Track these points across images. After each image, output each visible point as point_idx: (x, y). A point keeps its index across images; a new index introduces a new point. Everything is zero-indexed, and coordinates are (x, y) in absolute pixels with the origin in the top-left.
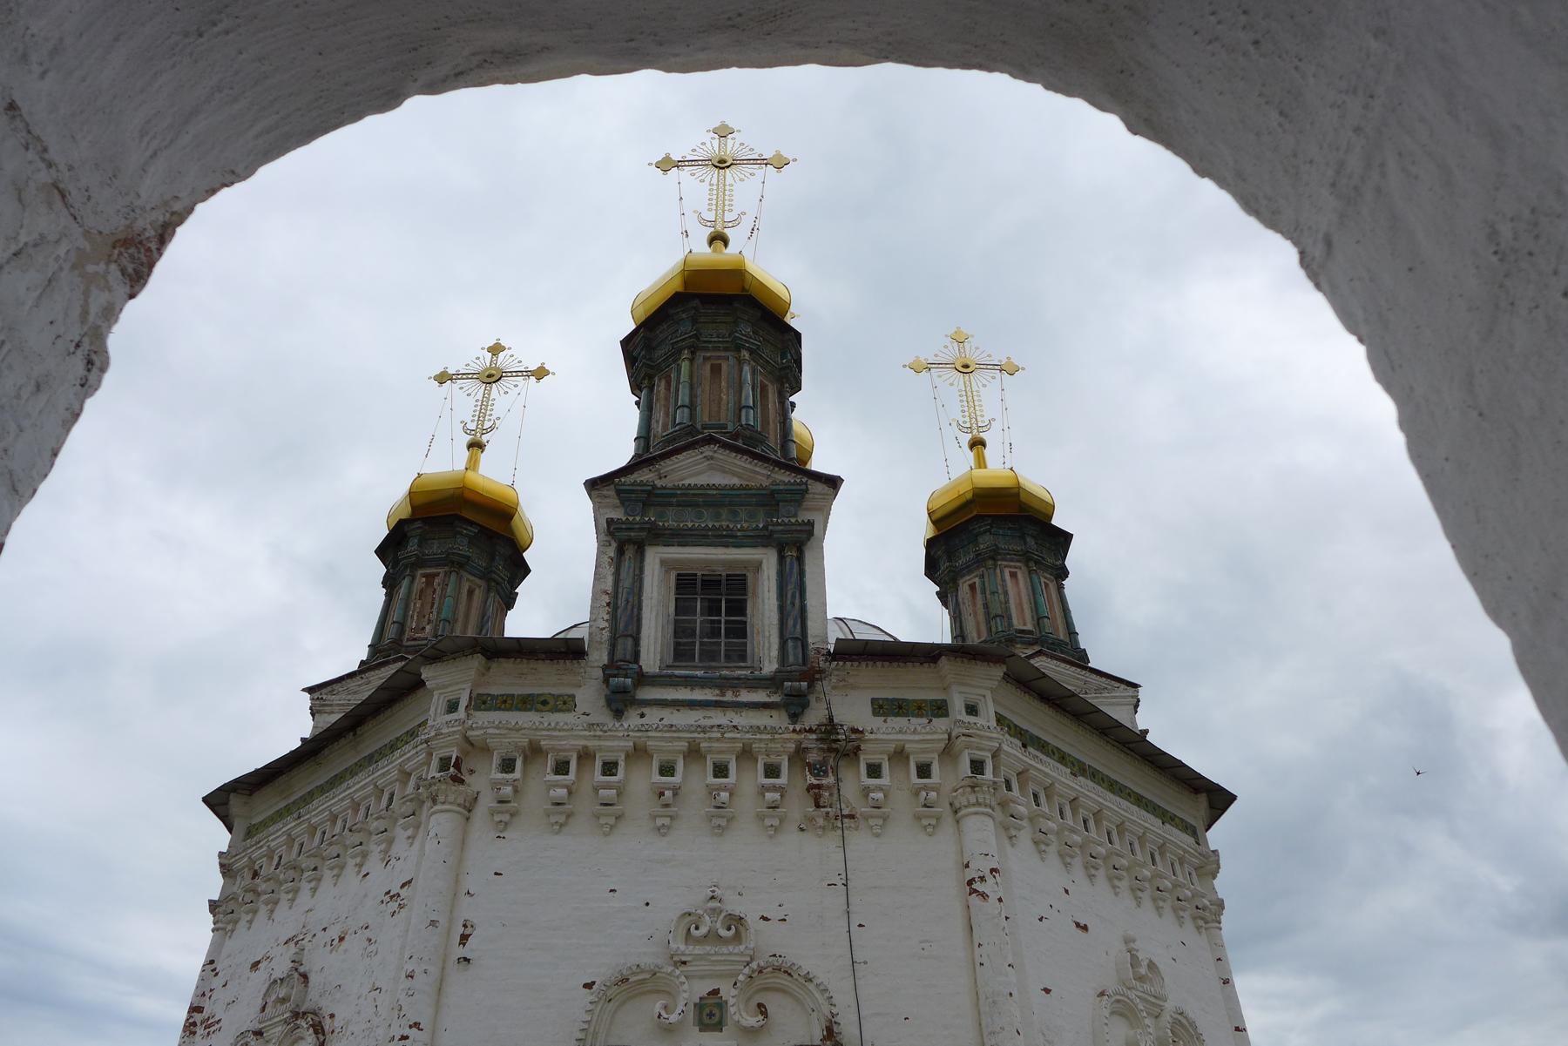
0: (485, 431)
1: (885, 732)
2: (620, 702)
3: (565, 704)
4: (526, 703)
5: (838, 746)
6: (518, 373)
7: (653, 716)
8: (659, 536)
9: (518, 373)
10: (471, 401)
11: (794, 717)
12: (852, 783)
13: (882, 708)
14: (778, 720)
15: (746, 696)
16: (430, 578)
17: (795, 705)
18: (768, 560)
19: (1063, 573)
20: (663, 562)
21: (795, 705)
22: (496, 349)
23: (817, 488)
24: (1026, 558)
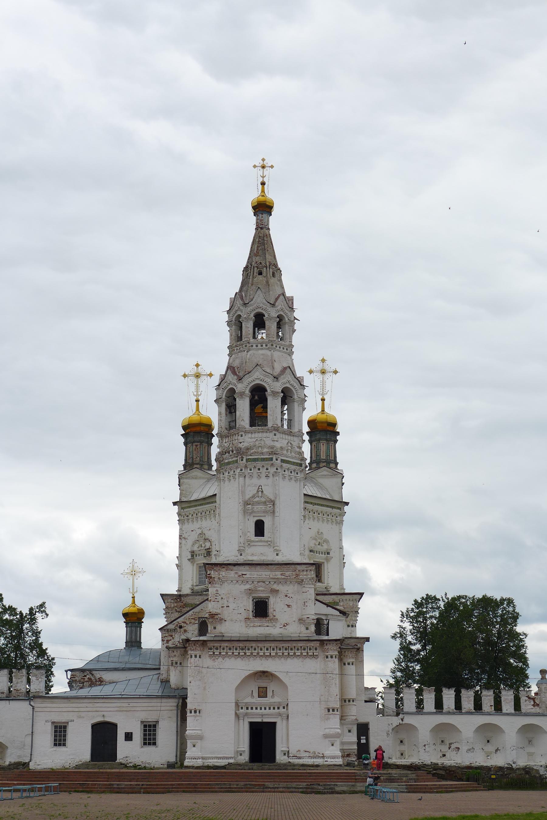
0: (199, 395)
6: (204, 375)
9: (204, 375)
10: (193, 384)
16: (196, 446)
19: (336, 441)
22: (197, 365)
24: (326, 440)
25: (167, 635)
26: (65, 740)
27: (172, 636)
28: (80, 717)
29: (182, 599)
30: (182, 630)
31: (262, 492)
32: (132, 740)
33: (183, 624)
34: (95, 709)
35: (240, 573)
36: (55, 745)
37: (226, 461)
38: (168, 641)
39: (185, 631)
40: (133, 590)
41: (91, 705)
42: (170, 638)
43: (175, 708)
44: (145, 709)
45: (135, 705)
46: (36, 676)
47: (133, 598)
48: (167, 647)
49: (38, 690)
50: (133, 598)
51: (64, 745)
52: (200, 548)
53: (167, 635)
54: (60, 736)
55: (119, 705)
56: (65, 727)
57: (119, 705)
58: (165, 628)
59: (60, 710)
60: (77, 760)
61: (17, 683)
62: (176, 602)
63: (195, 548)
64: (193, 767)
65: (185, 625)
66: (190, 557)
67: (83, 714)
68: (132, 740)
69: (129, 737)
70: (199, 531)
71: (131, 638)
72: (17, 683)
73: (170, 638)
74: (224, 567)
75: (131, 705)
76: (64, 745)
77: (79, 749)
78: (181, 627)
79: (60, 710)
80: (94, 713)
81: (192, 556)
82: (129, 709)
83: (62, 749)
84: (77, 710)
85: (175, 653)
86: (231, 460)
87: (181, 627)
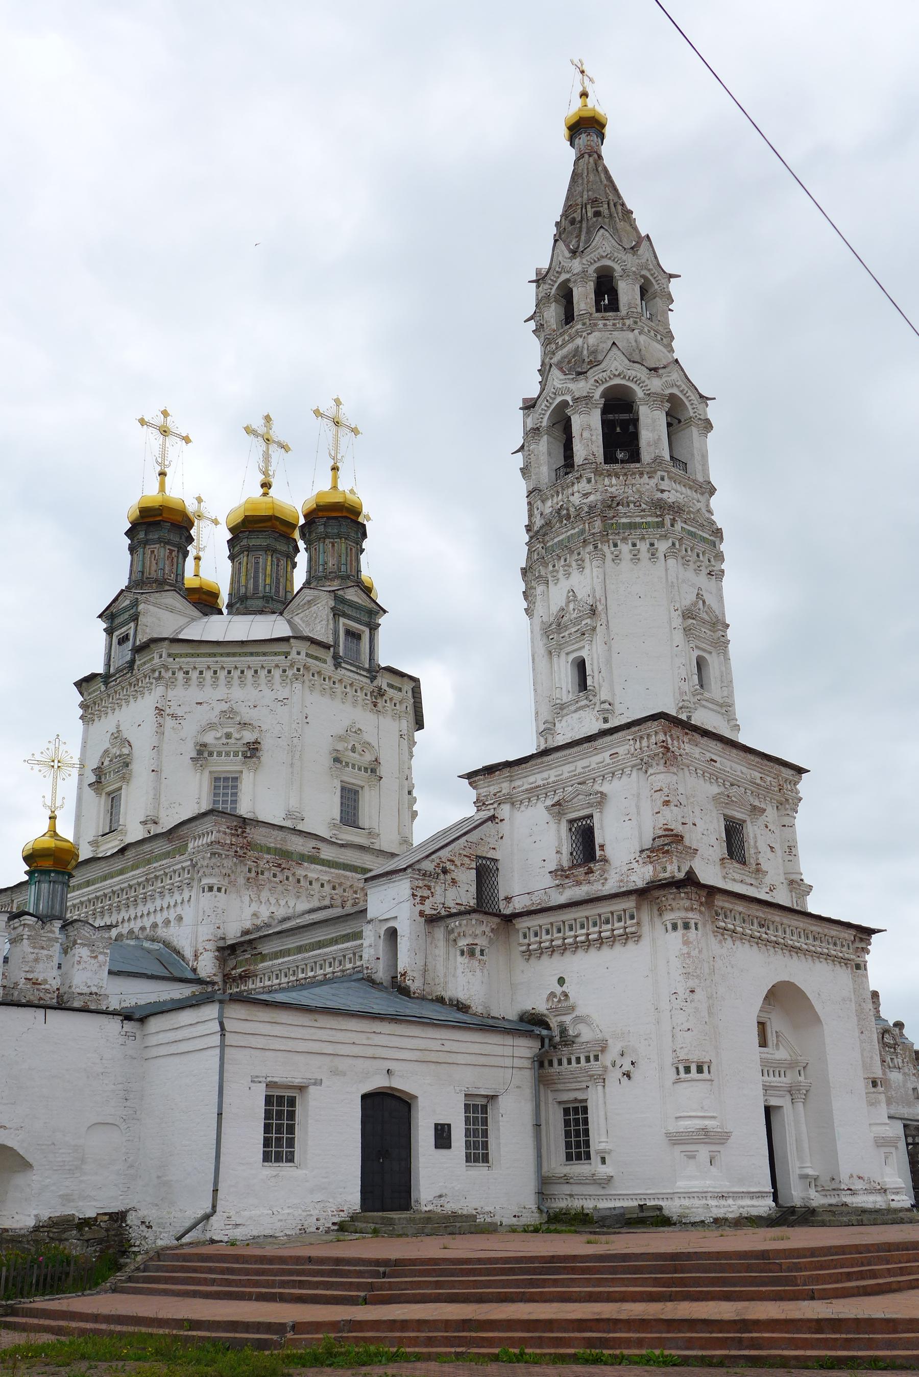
1: (391, 692)
2: (337, 665)
3: (325, 662)
4: (316, 658)
5: (381, 693)
7: (343, 671)
8: (345, 615)
11: (372, 682)
12: (381, 703)
13: (390, 686)
14: (368, 681)
15: (362, 672)
17: (373, 679)
18: (367, 631)
20: (344, 624)
21: (373, 679)
23: (381, 612)
25: (421, 884)
26: (291, 1143)
27: (429, 888)
28: (335, 1072)
29: (248, 831)
30: (448, 877)
31: (704, 602)
32: (449, 1147)
33: (449, 866)
34: (370, 1052)
35: (709, 756)
36: (267, 1158)
37: (624, 520)
38: (423, 899)
39: (454, 881)
40: (54, 799)
41: (361, 1039)
42: (426, 893)
43: (527, 1064)
44: (482, 1060)
45: (455, 1047)
46: (91, 945)
47: (53, 818)
48: (421, 914)
49: (94, 990)
50: (53, 818)
51: (290, 1159)
52: (224, 741)
53: (421, 884)
54: (279, 1130)
55: (421, 1044)
56: (292, 1102)
57: (421, 1044)
58: (417, 867)
59: (290, 1045)
60: (332, 1207)
61: (36, 960)
62: (232, 835)
63: (209, 738)
64: (726, 1219)
65: (453, 868)
66: (194, 754)
67: (342, 1064)
68: (449, 1147)
69: (442, 1137)
70: (225, 707)
71: (52, 908)
72: (36, 960)
73: (426, 893)
74: (687, 734)
75: (449, 1046)
76: (290, 1159)
77: (331, 1168)
78: (445, 871)
79: (290, 1045)
80: (368, 1062)
81: (200, 753)
82: (442, 1057)
83: (285, 1169)
84: (329, 1049)
85: (483, 928)
86: (638, 520)
87: (445, 871)
